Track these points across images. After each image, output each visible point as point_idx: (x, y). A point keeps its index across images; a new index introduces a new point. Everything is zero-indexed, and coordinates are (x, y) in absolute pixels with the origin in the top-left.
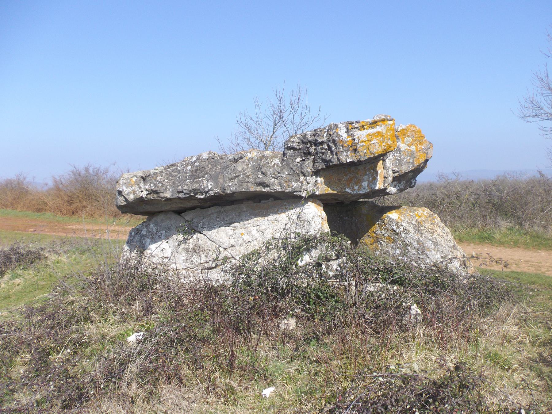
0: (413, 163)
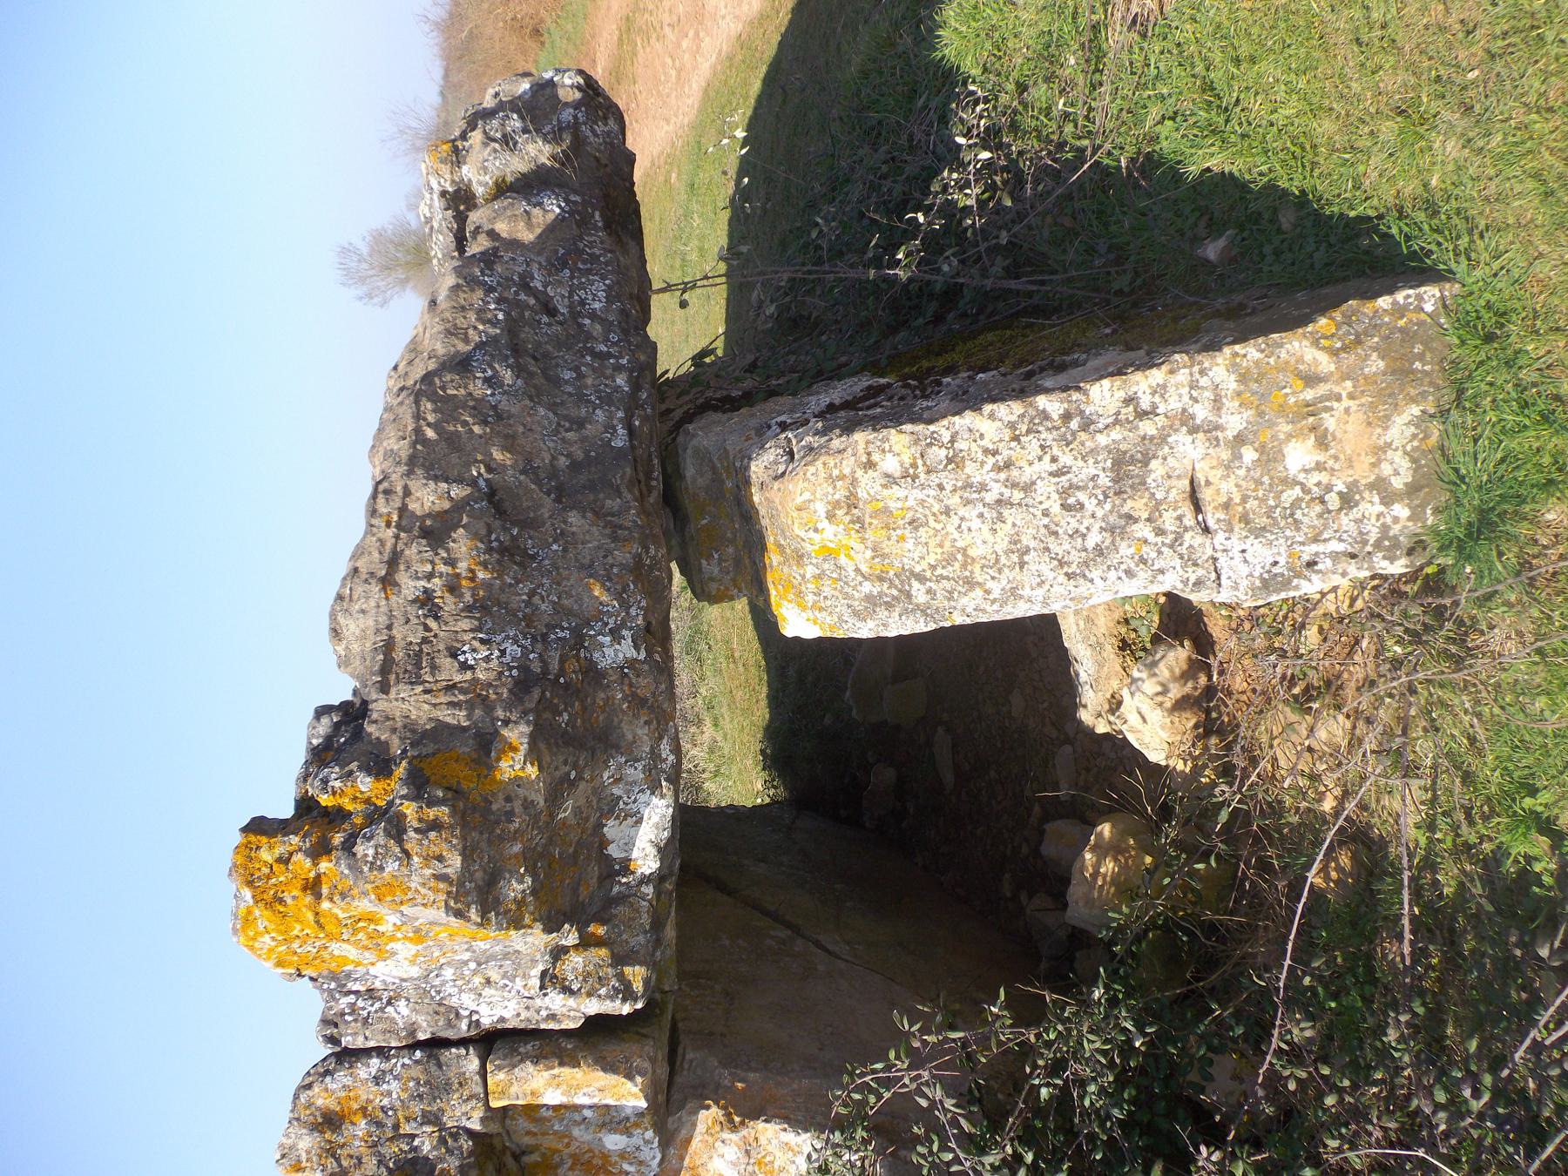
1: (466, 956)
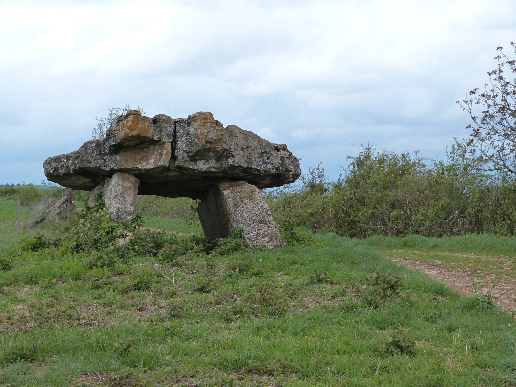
0: (198, 144)
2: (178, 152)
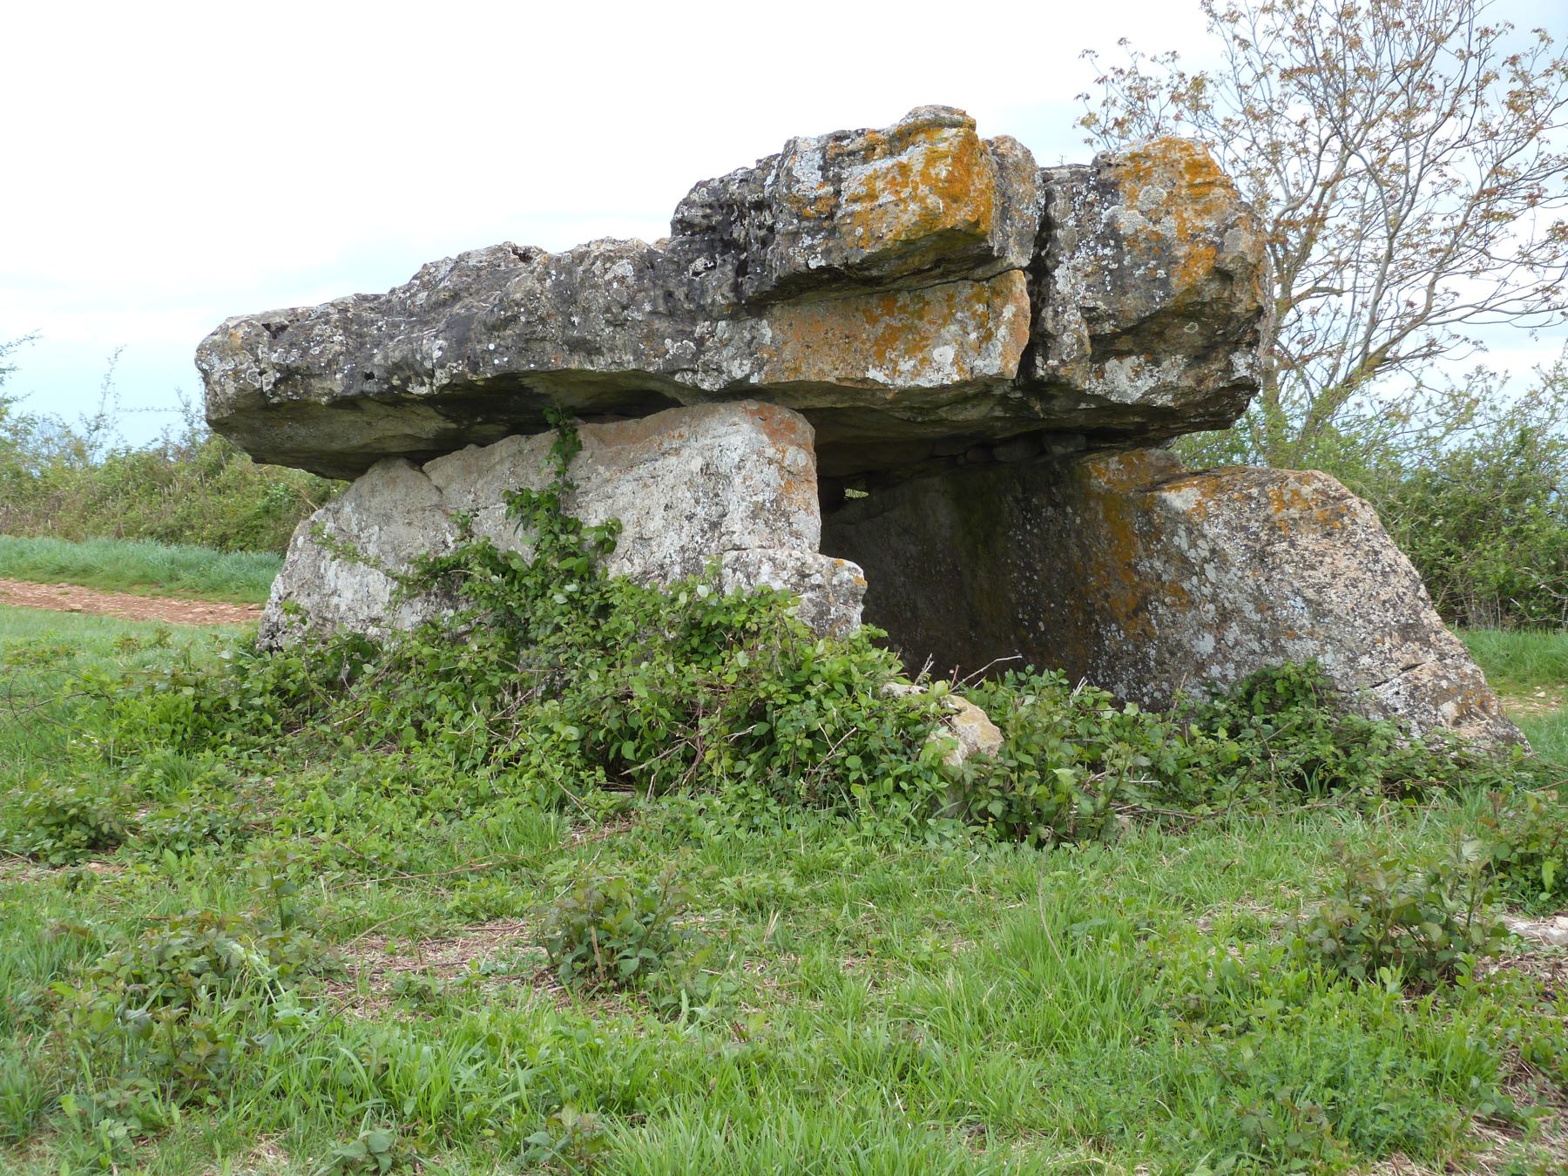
0: (1164, 283)
1: (1127, 261)
2: (1056, 313)
